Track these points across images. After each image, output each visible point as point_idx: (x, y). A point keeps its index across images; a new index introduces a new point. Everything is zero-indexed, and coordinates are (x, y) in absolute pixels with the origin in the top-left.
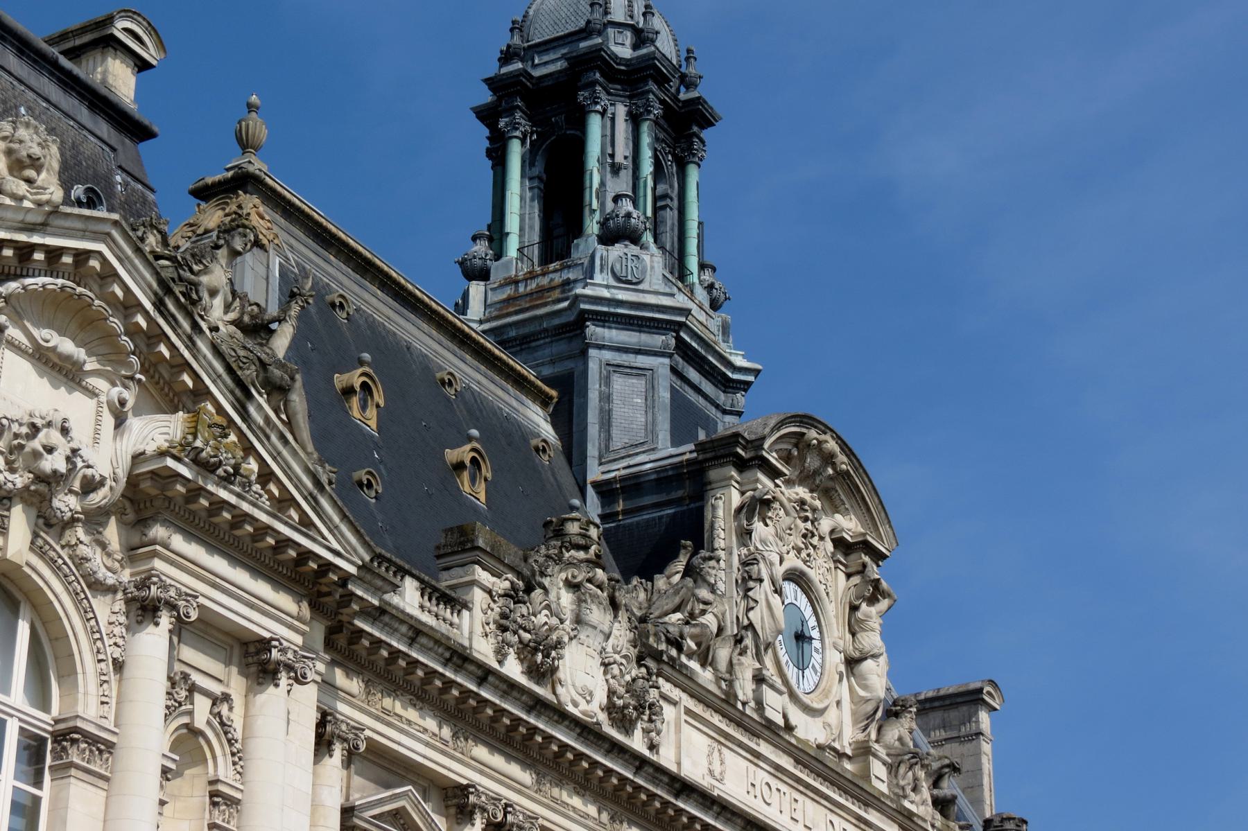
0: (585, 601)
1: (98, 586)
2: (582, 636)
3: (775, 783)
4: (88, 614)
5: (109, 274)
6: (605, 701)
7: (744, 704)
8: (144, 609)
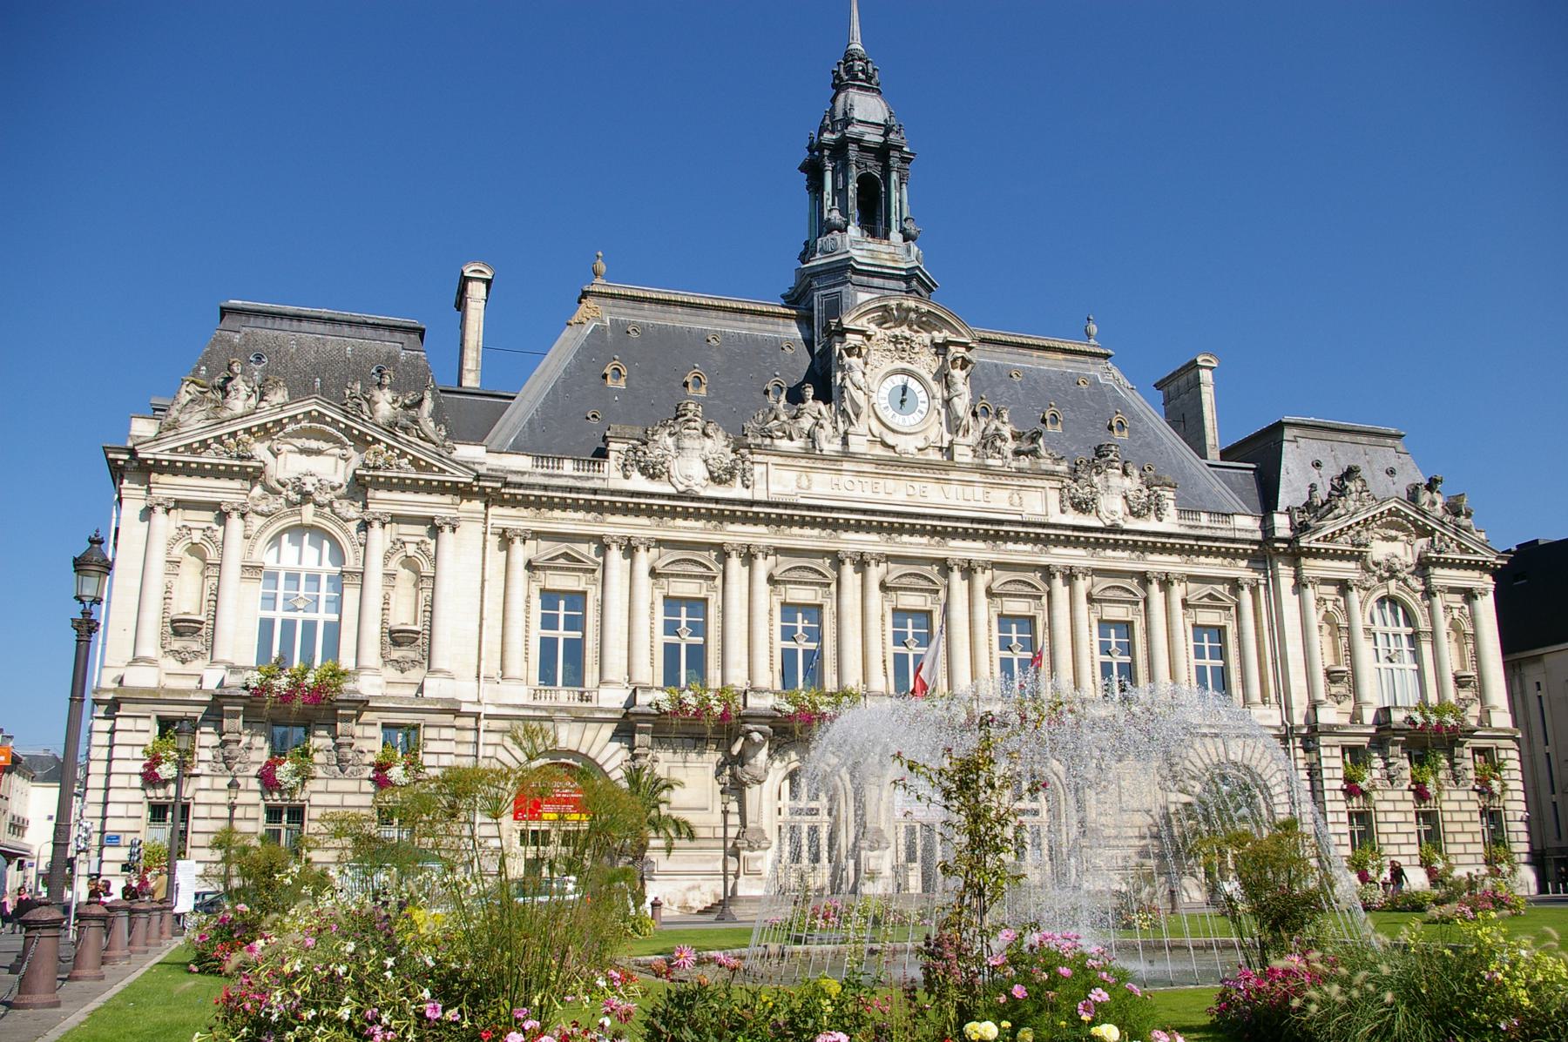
1: (347, 520)
3: (855, 479)
4: (346, 531)
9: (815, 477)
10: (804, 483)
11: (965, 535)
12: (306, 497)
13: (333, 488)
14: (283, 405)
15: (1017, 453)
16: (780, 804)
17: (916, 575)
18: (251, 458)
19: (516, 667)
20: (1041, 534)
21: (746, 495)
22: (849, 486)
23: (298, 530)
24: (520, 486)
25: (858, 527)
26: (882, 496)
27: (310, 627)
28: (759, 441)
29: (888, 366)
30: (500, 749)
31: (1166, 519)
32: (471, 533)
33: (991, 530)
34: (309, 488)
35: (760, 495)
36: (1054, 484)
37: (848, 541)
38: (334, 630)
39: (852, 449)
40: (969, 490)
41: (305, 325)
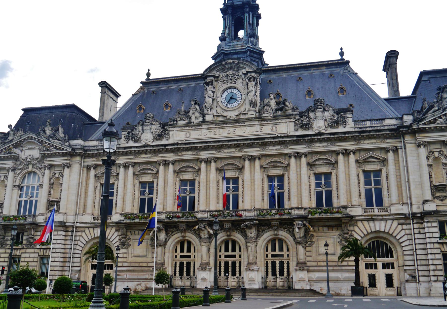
1: (40, 168)
3: (207, 131)
4: (40, 172)
5: (32, 137)
6: (153, 138)
8: (45, 168)
9: (192, 132)
10: (188, 135)
11: (251, 146)
12: (29, 163)
13: (37, 159)
14: (21, 136)
15: (277, 110)
16: (176, 254)
17: (229, 164)
18: (12, 153)
19: (89, 210)
20: (284, 141)
21: (167, 142)
22: (205, 134)
23: (29, 173)
24: (90, 150)
25: (207, 148)
27: (31, 202)
28: (172, 123)
29: (225, 86)
30: (81, 237)
31: (348, 126)
32: (76, 168)
33: (260, 142)
34: (28, 160)
36: (292, 120)
38: (36, 201)
39: (207, 120)
40: (254, 128)
41: (43, 111)
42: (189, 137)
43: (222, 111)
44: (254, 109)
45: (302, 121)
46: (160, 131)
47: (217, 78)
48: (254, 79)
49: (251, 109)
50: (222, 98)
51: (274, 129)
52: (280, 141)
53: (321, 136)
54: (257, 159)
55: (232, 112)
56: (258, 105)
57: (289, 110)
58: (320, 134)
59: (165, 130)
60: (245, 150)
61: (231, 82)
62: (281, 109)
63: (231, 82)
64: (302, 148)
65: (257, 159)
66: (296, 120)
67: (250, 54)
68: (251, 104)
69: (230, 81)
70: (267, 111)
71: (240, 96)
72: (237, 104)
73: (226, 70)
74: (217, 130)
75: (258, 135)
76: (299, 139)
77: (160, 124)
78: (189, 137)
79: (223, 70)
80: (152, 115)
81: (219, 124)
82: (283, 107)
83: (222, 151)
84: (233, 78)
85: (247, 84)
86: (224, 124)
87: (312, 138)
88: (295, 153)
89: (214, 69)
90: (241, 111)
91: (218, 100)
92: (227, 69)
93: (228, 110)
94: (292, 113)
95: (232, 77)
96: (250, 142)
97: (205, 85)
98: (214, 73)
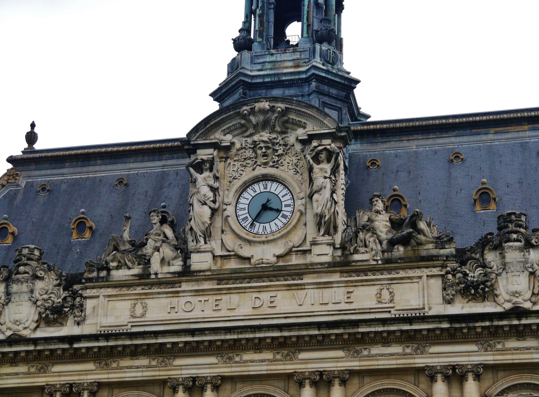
0: (10, 285)
2: (12, 299)
3: (195, 300)
6: (36, 317)
7: (156, 274)
9: (150, 302)
10: (139, 310)
11: (321, 343)
15: (392, 243)
20: (414, 330)
21: (76, 331)
22: (188, 307)
25: (193, 350)
26: (224, 313)
28: (95, 274)
29: (248, 174)
35: (87, 329)
36: (436, 271)
37: (181, 367)
40: (327, 294)
42: (143, 315)
43: (239, 242)
44: (327, 239)
45: (465, 275)
46: (58, 297)
47: (225, 150)
48: (330, 155)
49: (320, 239)
50: (240, 206)
51: (386, 294)
52: (402, 331)
53: (519, 319)
54: (337, 382)
55: (266, 247)
56: (341, 228)
57: (428, 243)
58: (518, 312)
59: (75, 295)
60: (303, 355)
61: (266, 164)
62: (405, 241)
63: (266, 164)
64: (466, 354)
65: (337, 382)
66: (448, 273)
67: (317, 87)
68: (319, 225)
69: (262, 160)
70: (366, 246)
71: (290, 202)
72: (280, 225)
73: (251, 131)
74: (224, 297)
75: (340, 312)
76: (457, 325)
77: (60, 276)
78: (143, 315)
79: (242, 130)
80: (37, 253)
81: (229, 279)
82: (410, 235)
83: (237, 359)
84: (269, 151)
85: (311, 170)
86: (242, 279)
87: (496, 323)
88: (446, 367)
89: (217, 125)
90: (291, 244)
91: (226, 213)
92: (255, 127)
93: (255, 242)
94: (435, 252)
95: (267, 148)
96: (316, 332)
97: (191, 170)
98: (217, 136)
